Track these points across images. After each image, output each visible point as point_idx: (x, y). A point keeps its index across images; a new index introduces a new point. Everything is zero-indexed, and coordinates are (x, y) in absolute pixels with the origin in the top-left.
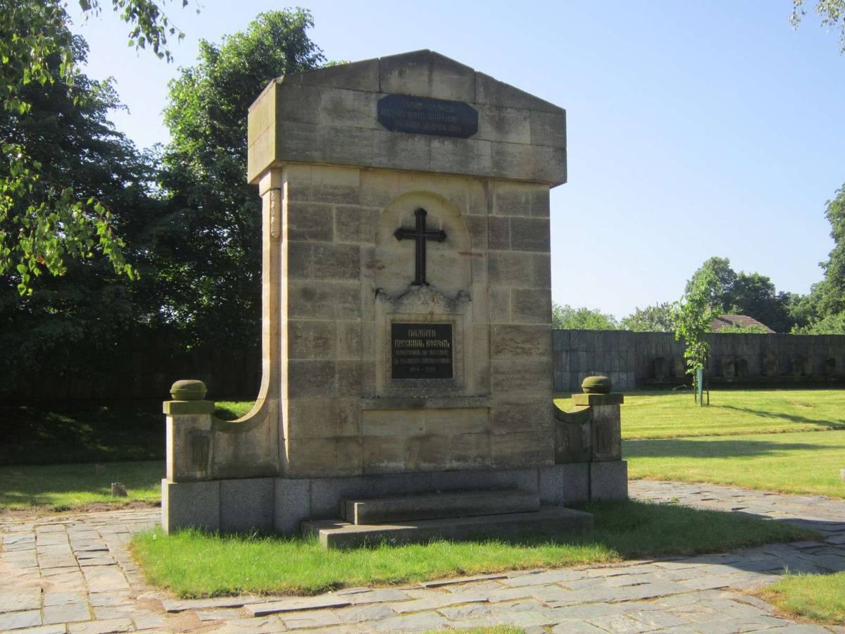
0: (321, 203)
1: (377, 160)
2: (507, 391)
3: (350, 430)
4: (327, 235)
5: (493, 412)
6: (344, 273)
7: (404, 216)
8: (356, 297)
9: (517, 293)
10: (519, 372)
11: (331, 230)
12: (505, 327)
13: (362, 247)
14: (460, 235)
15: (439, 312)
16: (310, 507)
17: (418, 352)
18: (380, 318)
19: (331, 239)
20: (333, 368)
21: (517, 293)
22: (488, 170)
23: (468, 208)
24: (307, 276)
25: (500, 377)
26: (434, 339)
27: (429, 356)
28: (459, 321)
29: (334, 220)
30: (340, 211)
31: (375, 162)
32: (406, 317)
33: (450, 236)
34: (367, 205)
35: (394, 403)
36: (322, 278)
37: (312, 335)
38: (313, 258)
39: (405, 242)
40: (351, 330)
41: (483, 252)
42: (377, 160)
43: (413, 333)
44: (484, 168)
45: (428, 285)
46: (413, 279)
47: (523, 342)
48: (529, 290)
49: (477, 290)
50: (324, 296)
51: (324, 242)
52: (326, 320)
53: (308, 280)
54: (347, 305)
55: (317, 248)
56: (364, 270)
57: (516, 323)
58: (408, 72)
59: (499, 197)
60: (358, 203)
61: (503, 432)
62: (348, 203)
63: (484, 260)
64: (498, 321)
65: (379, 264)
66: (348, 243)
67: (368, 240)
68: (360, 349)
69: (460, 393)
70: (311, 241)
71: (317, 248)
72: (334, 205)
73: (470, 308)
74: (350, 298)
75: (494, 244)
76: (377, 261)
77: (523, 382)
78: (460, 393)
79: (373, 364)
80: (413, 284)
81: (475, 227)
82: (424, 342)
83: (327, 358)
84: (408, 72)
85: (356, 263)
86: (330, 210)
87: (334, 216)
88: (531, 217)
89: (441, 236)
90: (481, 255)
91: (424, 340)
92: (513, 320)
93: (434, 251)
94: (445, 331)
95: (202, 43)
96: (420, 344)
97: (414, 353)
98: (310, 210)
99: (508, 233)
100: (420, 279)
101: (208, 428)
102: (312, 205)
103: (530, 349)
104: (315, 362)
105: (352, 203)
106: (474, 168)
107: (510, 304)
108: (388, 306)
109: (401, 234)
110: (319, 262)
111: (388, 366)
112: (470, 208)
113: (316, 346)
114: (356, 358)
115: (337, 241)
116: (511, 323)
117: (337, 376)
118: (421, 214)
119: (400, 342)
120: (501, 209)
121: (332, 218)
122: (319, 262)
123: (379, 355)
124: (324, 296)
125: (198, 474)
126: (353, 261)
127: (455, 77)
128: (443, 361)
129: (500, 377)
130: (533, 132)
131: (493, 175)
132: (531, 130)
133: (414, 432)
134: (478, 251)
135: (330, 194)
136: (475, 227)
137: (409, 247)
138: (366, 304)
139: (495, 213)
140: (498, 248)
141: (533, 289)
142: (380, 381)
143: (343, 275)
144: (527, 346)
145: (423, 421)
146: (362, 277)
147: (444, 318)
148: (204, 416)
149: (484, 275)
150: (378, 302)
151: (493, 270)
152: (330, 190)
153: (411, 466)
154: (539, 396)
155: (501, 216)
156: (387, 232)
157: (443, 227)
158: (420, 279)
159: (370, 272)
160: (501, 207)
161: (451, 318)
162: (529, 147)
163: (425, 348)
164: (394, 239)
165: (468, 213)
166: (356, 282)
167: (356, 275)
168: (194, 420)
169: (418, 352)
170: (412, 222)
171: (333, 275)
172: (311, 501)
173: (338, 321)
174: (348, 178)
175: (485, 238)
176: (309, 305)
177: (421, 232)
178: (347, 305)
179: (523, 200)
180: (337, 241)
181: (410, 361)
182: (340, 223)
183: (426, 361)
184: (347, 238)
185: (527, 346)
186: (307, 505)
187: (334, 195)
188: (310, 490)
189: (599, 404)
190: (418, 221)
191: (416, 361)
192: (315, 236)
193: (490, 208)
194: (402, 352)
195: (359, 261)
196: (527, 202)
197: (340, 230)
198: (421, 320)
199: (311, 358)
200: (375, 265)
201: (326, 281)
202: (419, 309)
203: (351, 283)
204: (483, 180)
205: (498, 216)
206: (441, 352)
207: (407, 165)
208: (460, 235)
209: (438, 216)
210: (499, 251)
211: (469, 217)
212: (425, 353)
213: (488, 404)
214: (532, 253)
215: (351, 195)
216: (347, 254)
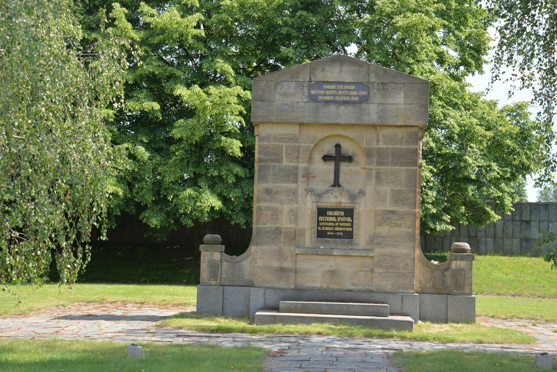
0: (277, 143)
1: (307, 119)
2: (384, 248)
3: (287, 264)
4: (280, 161)
5: (375, 259)
6: (289, 180)
7: (329, 148)
8: (295, 193)
9: (393, 191)
10: (392, 237)
11: (282, 157)
12: (384, 211)
13: (300, 166)
14: (361, 158)
15: (345, 202)
16: (264, 303)
17: (332, 224)
18: (309, 206)
19: (282, 162)
20: (281, 231)
21: (393, 191)
22: (375, 121)
23: (365, 142)
24: (268, 182)
25: (380, 240)
26: (342, 217)
27: (339, 226)
28: (357, 207)
29: (284, 152)
30: (287, 147)
31: (306, 120)
32: (324, 204)
33: (356, 159)
34: (304, 143)
35: (314, 252)
36: (276, 183)
37: (270, 213)
38: (271, 173)
39: (328, 162)
40: (291, 211)
41: (373, 167)
42: (307, 119)
43: (330, 213)
44: (372, 120)
45: (340, 186)
46: (332, 183)
47: (396, 220)
48: (402, 190)
49: (369, 190)
50: (277, 193)
51: (278, 164)
52: (277, 205)
53: (269, 184)
54: (290, 198)
55: (274, 167)
56: (300, 179)
57: (392, 209)
58: (327, 68)
59: (383, 136)
60: (298, 143)
61: (381, 271)
62: (292, 143)
63: (374, 172)
64: (380, 208)
65: (313, 175)
66: (291, 164)
67: (304, 162)
68: (296, 220)
69: (356, 247)
70: (271, 164)
71: (274, 167)
72: (284, 144)
73: (363, 200)
74: (291, 194)
75: (379, 164)
76: (311, 173)
77: (395, 243)
78: (356, 247)
79: (304, 230)
80: (332, 186)
81: (369, 154)
82: (336, 218)
83: (278, 226)
84: (327, 68)
85: (296, 175)
86: (282, 147)
87: (284, 150)
88: (404, 146)
89: (350, 159)
90: (372, 169)
91: (336, 217)
92: (390, 207)
93: (344, 167)
94: (349, 212)
95: (124, 85)
96: (335, 220)
97: (330, 224)
98: (271, 147)
99: (388, 157)
100: (336, 184)
101: (219, 259)
102: (272, 145)
103: (401, 224)
104: (271, 227)
105: (289, 142)
106: (366, 120)
107: (388, 198)
108: (314, 198)
109: (326, 158)
110: (275, 175)
111: (313, 230)
112: (366, 142)
113: (272, 219)
114: (293, 226)
115: (285, 163)
116: (389, 209)
117: (283, 235)
118: (338, 146)
119: (321, 218)
120: (385, 142)
121: (283, 151)
122: (275, 175)
123: (307, 223)
124: (277, 193)
125: (213, 283)
126: (294, 174)
127: (356, 68)
128: (348, 229)
129: (380, 240)
130: (406, 97)
131: (378, 123)
132: (405, 95)
133: (328, 268)
134: (370, 167)
135: (282, 138)
136: (369, 154)
137: (330, 166)
138: (301, 197)
139: (380, 145)
140: (382, 165)
141: (403, 189)
142: (309, 239)
143: (288, 182)
144: (398, 222)
145: (330, 263)
146: (299, 182)
147: (348, 205)
148: (217, 253)
149: (374, 181)
150: (308, 196)
151: (379, 179)
152: (282, 136)
153: (325, 286)
154: (405, 251)
155: (384, 147)
156: (318, 157)
157: (352, 154)
158: (336, 184)
159: (305, 179)
160: (385, 141)
161: (352, 205)
162: (403, 105)
163: (337, 222)
164: (322, 160)
165: (365, 146)
166: (296, 185)
167: (296, 181)
168: (212, 255)
169: (332, 224)
170: (333, 152)
171: (282, 182)
172: (265, 300)
173: (284, 206)
174: (294, 130)
175: (375, 159)
176: (268, 197)
177: (338, 157)
178: (290, 198)
179: (400, 136)
180: (285, 163)
181: (327, 229)
182: (286, 153)
183: (337, 229)
184: (291, 162)
185: (398, 222)
186: (263, 302)
187: (284, 138)
188: (265, 294)
189: (455, 260)
190: (336, 150)
191: (331, 229)
192: (273, 161)
193: (378, 142)
194: (324, 224)
195: (297, 174)
196: (403, 138)
197: (286, 157)
198: (333, 206)
199: (269, 225)
200: (308, 175)
201: (278, 185)
202: (334, 199)
203: (293, 185)
204: (374, 126)
205: (383, 147)
206: (347, 224)
207: (325, 121)
208: (361, 158)
209: (347, 148)
210: (382, 167)
211: (365, 148)
212: (337, 224)
213: (371, 254)
214: (404, 168)
215: (294, 139)
216: (290, 170)
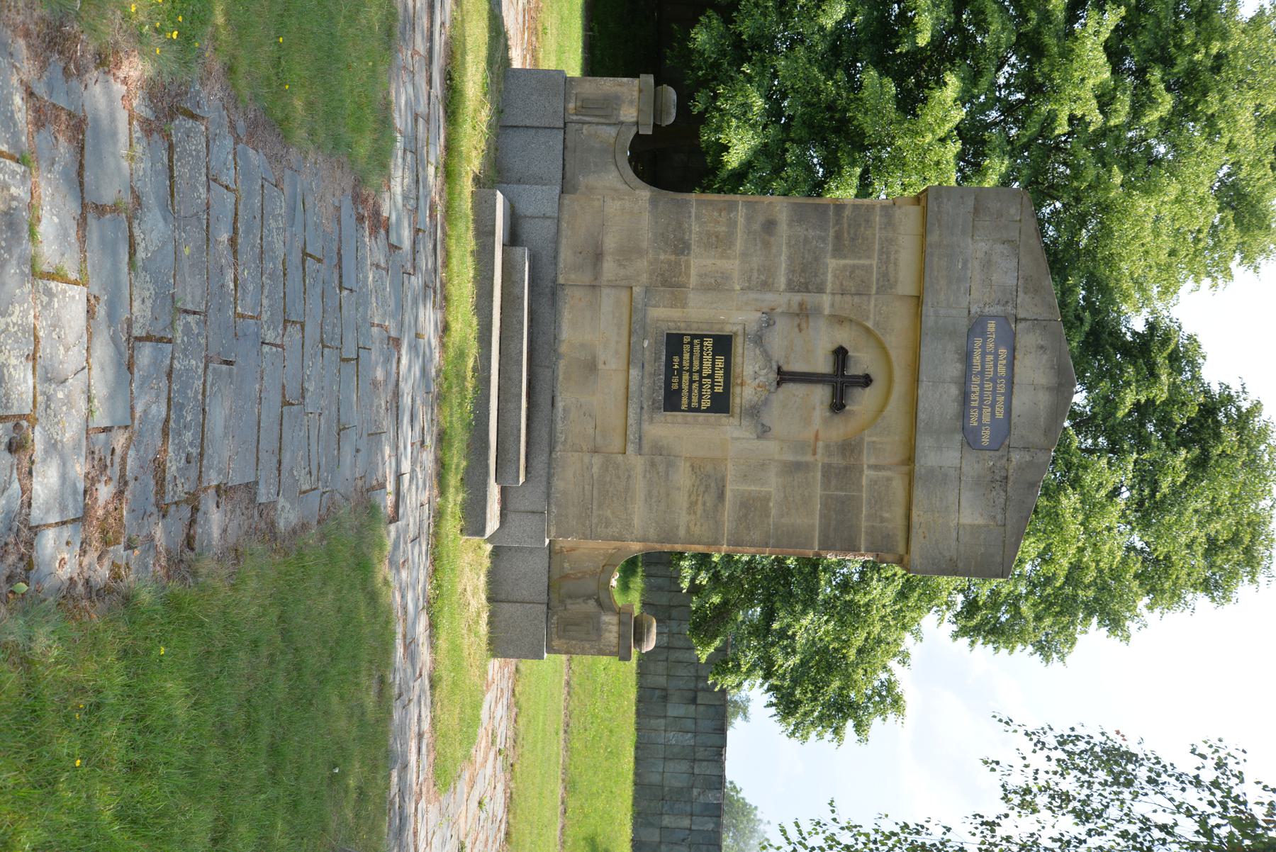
0: (877, 247)
2: (644, 477)
3: (609, 268)
4: (838, 251)
5: (620, 457)
6: (793, 271)
8: (766, 286)
10: (668, 495)
11: (845, 257)
12: (723, 479)
14: (839, 430)
15: (745, 394)
16: (526, 216)
17: (696, 368)
18: (735, 316)
19: (834, 256)
20: (682, 253)
21: (766, 499)
24: (790, 225)
25: (661, 469)
26: (712, 388)
27: (691, 382)
29: (856, 262)
30: (868, 269)
31: (928, 310)
32: (739, 350)
33: (838, 419)
35: (635, 326)
36: (788, 244)
38: (811, 233)
39: (831, 359)
40: (726, 277)
41: (819, 457)
43: (720, 362)
45: (779, 384)
47: (704, 504)
49: (771, 447)
50: (767, 245)
51: (830, 247)
52: (739, 245)
53: (785, 227)
54: (755, 275)
55: (824, 240)
56: (797, 298)
57: (728, 494)
58: (1045, 357)
59: (889, 479)
60: (877, 293)
61: (595, 469)
62: (878, 280)
63: (808, 458)
64: (731, 471)
65: (804, 325)
66: (830, 276)
67: (832, 305)
68: (705, 288)
69: (646, 417)
70: (832, 233)
71: (824, 240)
72: (875, 262)
73: (747, 435)
75: (827, 470)
76: (807, 322)
78: (646, 417)
79: (684, 306)
80: (779, 368)
81: (849, 448)
84: (1045, 357)
86: (869, 257)
87: (862, 262)
88: (864, 524)
89: (838, 406)
90: (814, 453)
91: (711, 376)
93: (820, 395)
94: (721, 404)
96: (706, 372)
97: (696, 363)
99: (841, 490)
100: (784, 377)
101: (622, 119)
103: (695, 513)
105: (878, 273)
106: (925, 443)
109: (841, 355)
110: (806, 240)
111: (683, 325)
114: (693, 280)
115: (832, 264)
117: (673, 258)
118: (866, 381)
119: (708, 343)
120: (873, 482)
121: (860, 258)
122: (806, 240)
123: (698, 312)
124: (767, 245)
125: (571, 106)
127: (1042, 421)
128: (685, 401)
129: (661, 469)
132: (979, 526)
133: (601, 357)
134: (820, 451)
135: (888, 257)
136: (849, 448)
137: (823, 365)
138: (757, 300)
139: (868, 474)
142: (665, 315)
144: (700, 507)
145: (612, 361)
146: (788, 295)
147: (738, 400)
148: (635, 114)
149: (790, 457)
150: (759, 314)
151: (795, 468)
153: (563, 349)
155: (864, 481)
156: (843, 337)
158: (784, 377)
159: (795, 308)
161: (737, 410)
163: (701, 377)
164: (836, 346)
165: (867, 439)
166: (783, 287)
167: (791, 288)
168: (631, 102)
169: (696, 368)
170: (854, 370)
171: (790, 258)
172: (532, 217)
173: (737, 262)
174: (906, 283)
175: (837, 461)
176: (756, 227)
178: (755, 275)
179: (886, 515)
180: (832, 264)
181: (686, 356)
182: (854, 267)
183: (686, 377)
184: (835, 276)
185: (700, 507)
186: (528, 214)
188: (545, 217)
189: (620, 623)
191: (686, 364)
192: (838, 237)
193: (875, 467)
196: (883, 520)
197: (845, 266)
198: (736, 370)
199: (695, 228)
200: (803, 314)
201: (784, 248)
202: (750, 370)
203: (782, 281)
204: (910, 459)
206: (695, 399)
207: (925, 352)
208: (839, 430)
209: (863, 402)
211: (862, 439)
212: (696, 377)
213: (631, 448)
215: (887, 283)
216: (816, 276)
